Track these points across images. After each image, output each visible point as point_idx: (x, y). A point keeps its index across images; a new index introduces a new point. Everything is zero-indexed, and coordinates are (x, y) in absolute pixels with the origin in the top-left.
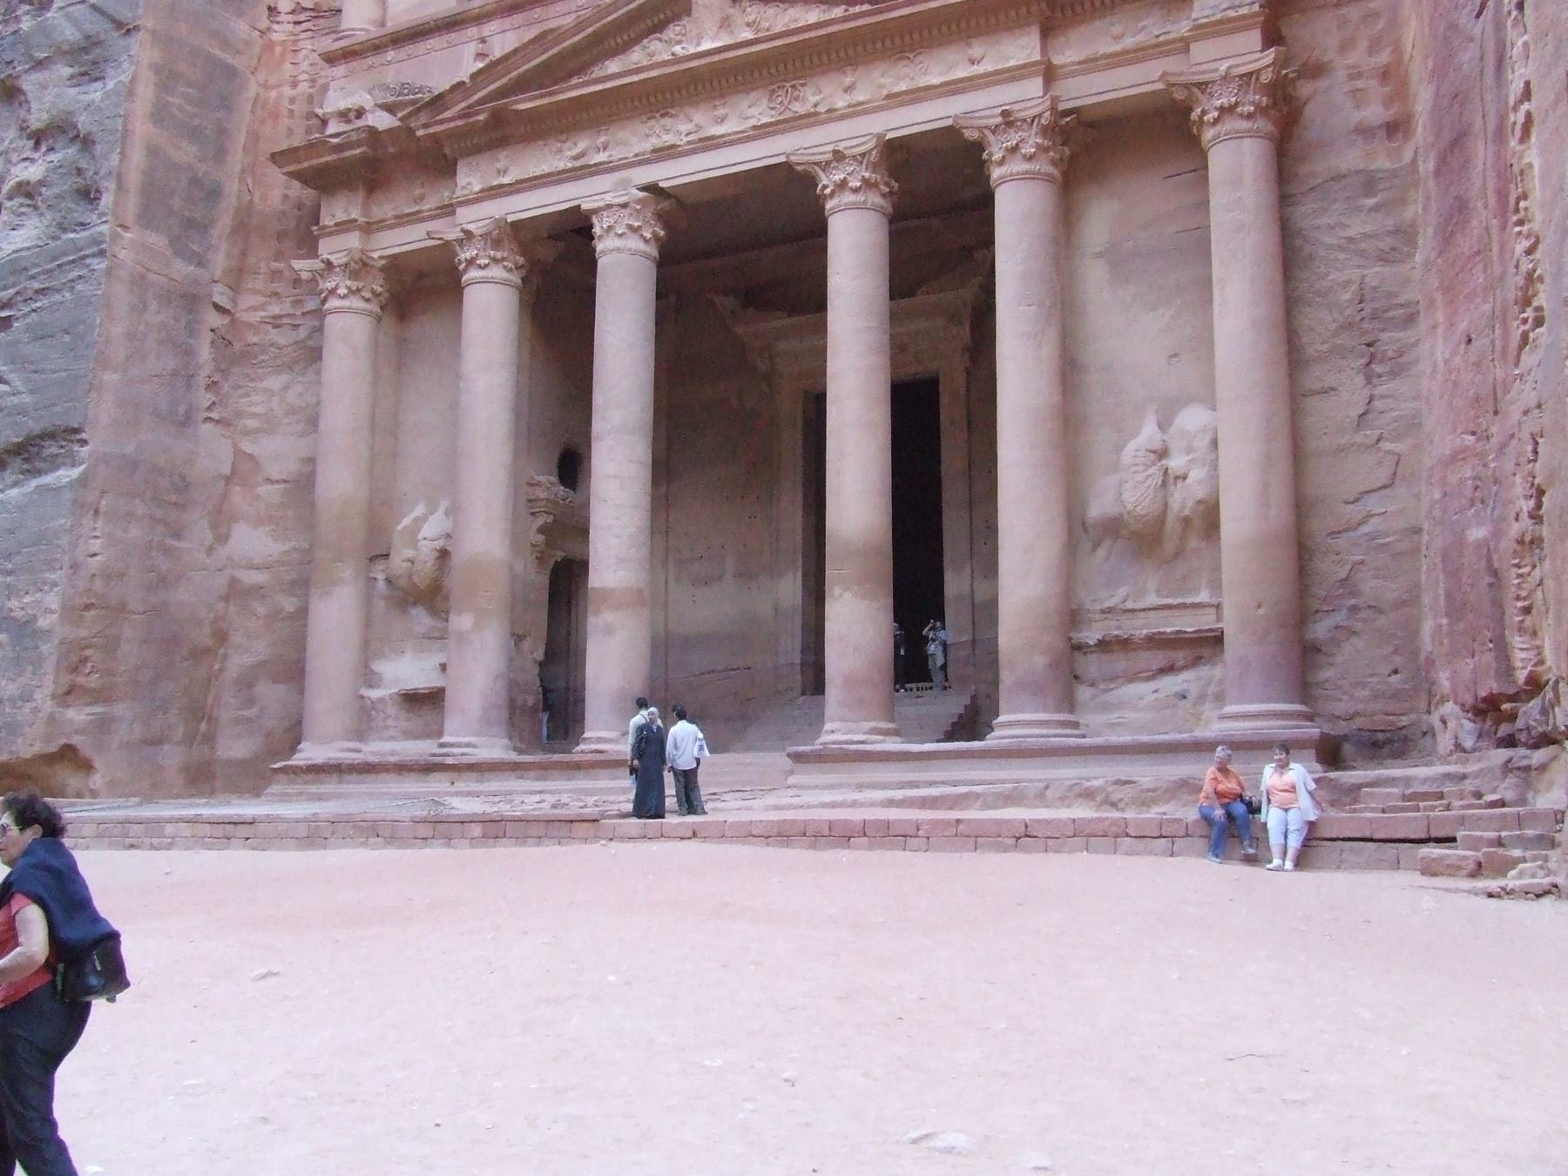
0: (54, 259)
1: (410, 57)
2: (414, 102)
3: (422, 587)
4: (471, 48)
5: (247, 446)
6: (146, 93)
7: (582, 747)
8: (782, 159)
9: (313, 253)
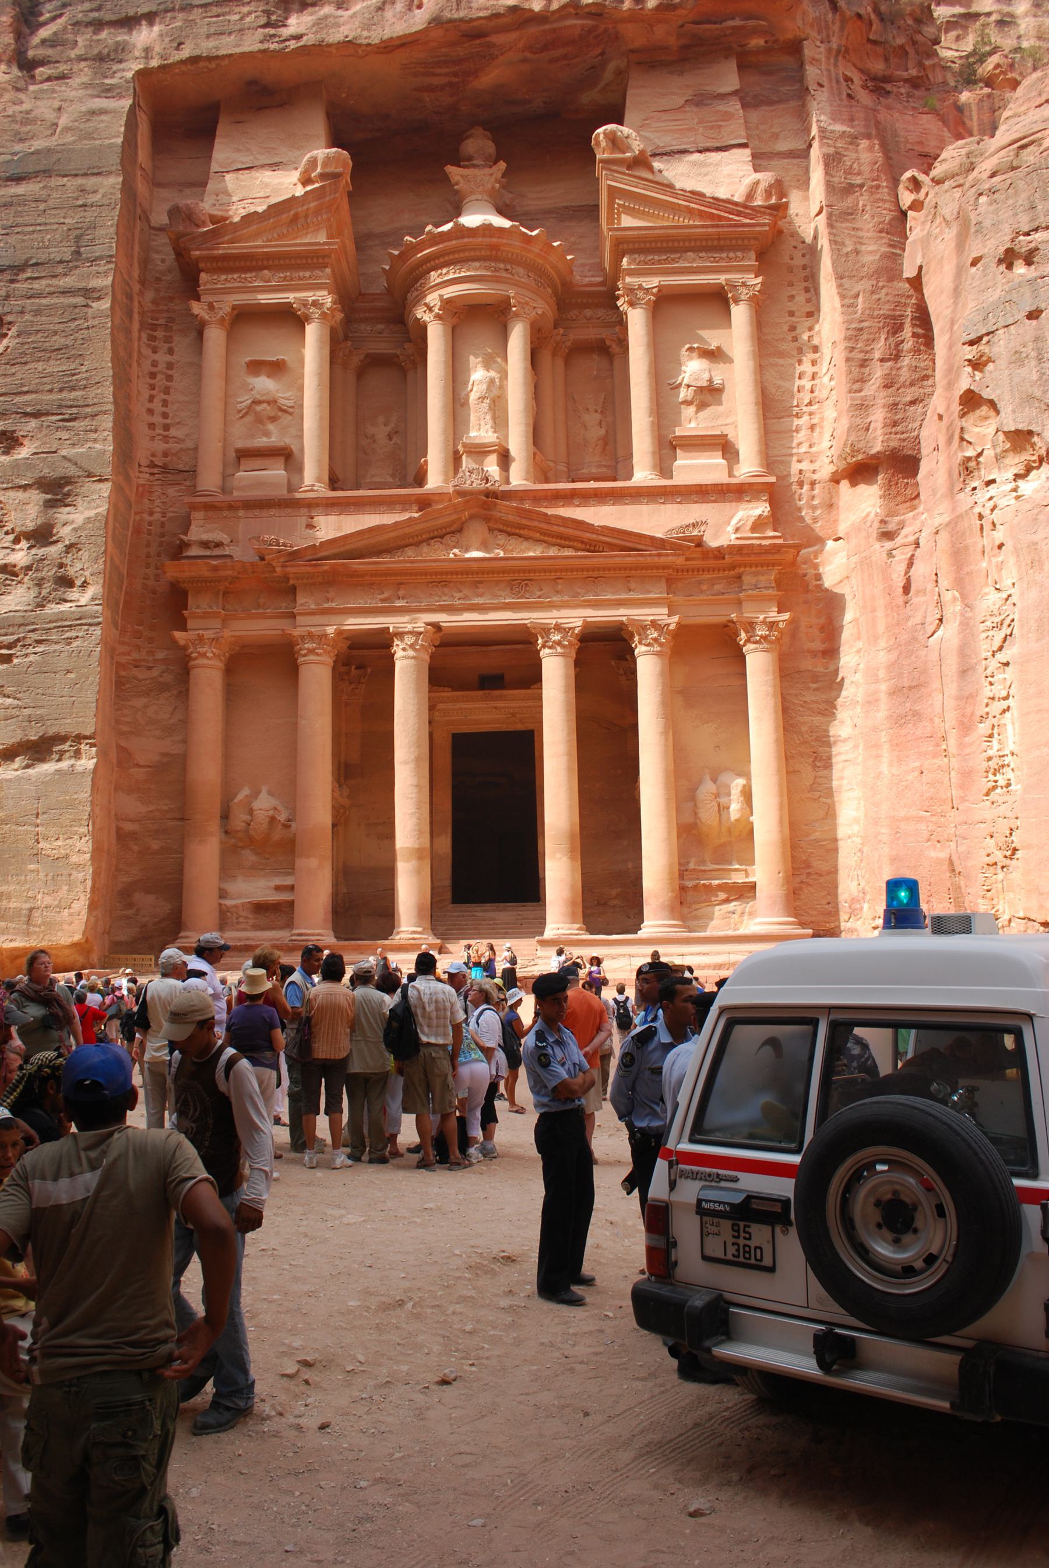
0: (50, 622)
1: (256, 517)
2: (280, 551)
4: (303, 521)
5: (124, 744)
7: (398, 937)
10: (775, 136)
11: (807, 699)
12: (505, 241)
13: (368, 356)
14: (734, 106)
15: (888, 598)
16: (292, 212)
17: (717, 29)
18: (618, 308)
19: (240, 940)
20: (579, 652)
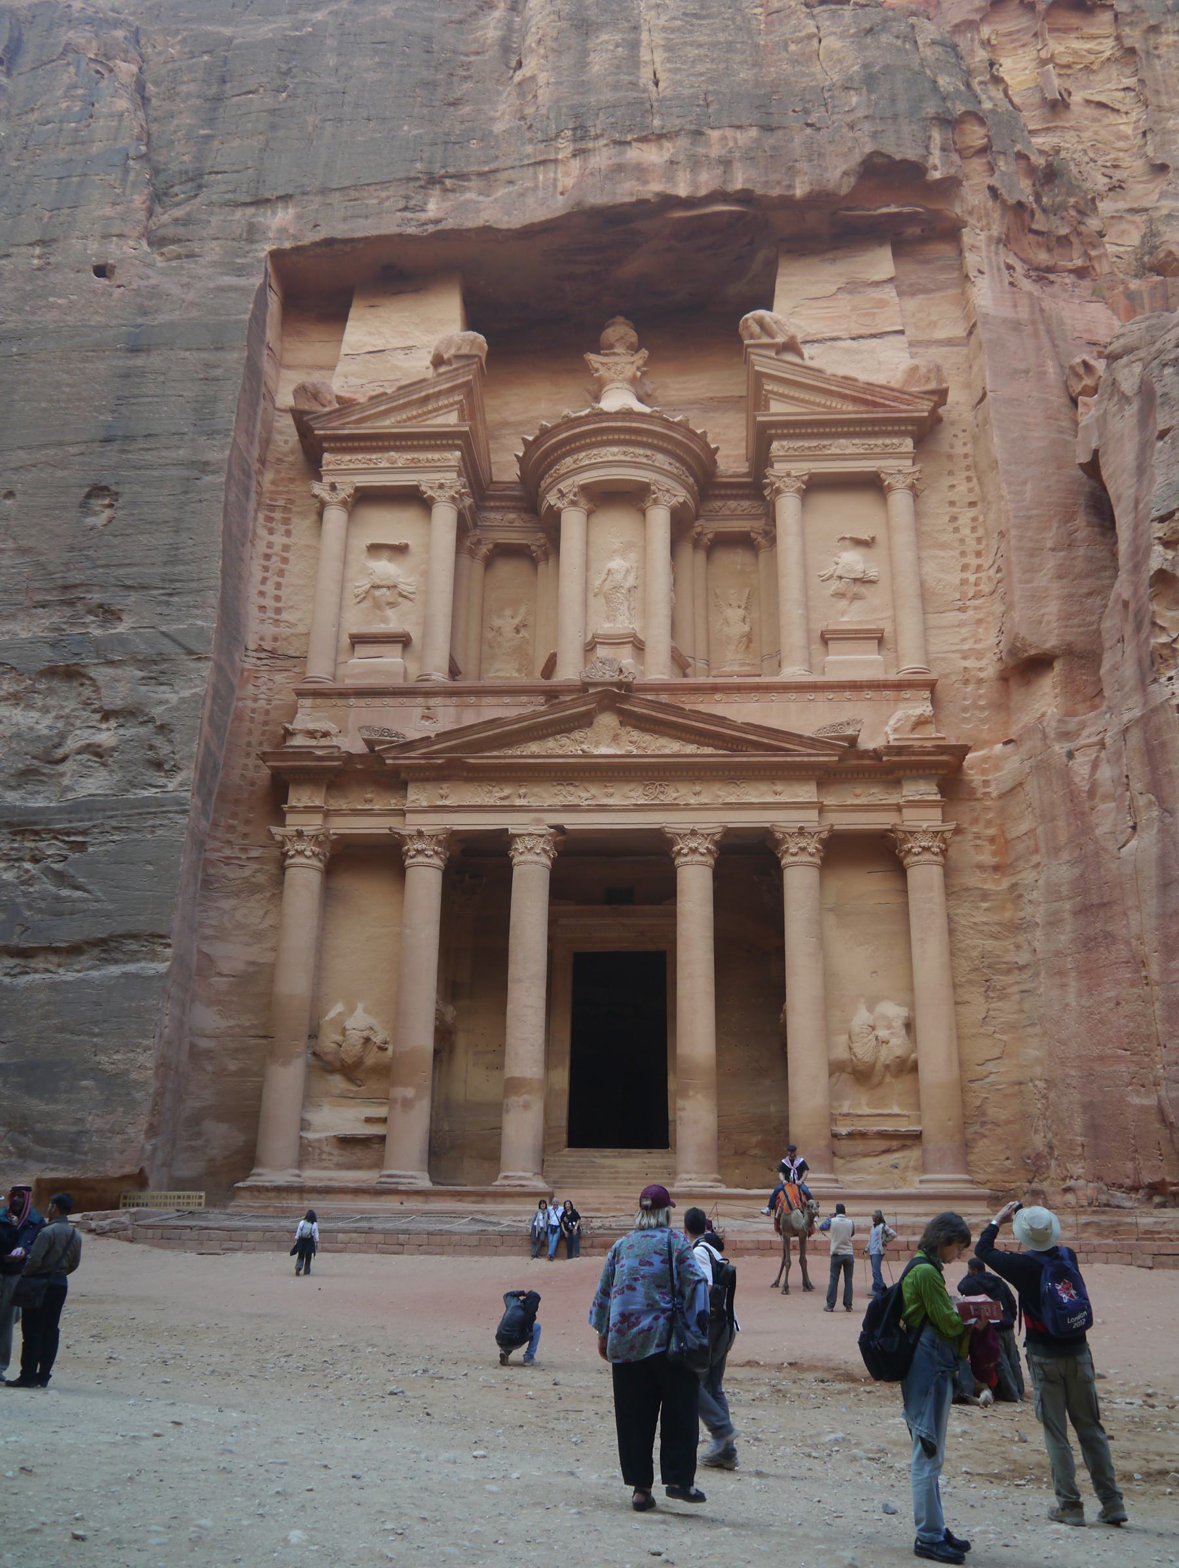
1: (368, 706)
2: (391, 742)
3: (349, 1061)
4: (419, 711)
5: (206, 949)
6: (208, 701)
8: (658, 826)
9: (281, 823)
10: (933, 324)
11: (974, 920)
12: (645, 426)
13: (497, 546)
14: (889, 293)
15: (1069, 805)
16: (423, 394)
17: (872, 216)
18: (763, 498)
19: (321, 1180)
20: (717, 862)
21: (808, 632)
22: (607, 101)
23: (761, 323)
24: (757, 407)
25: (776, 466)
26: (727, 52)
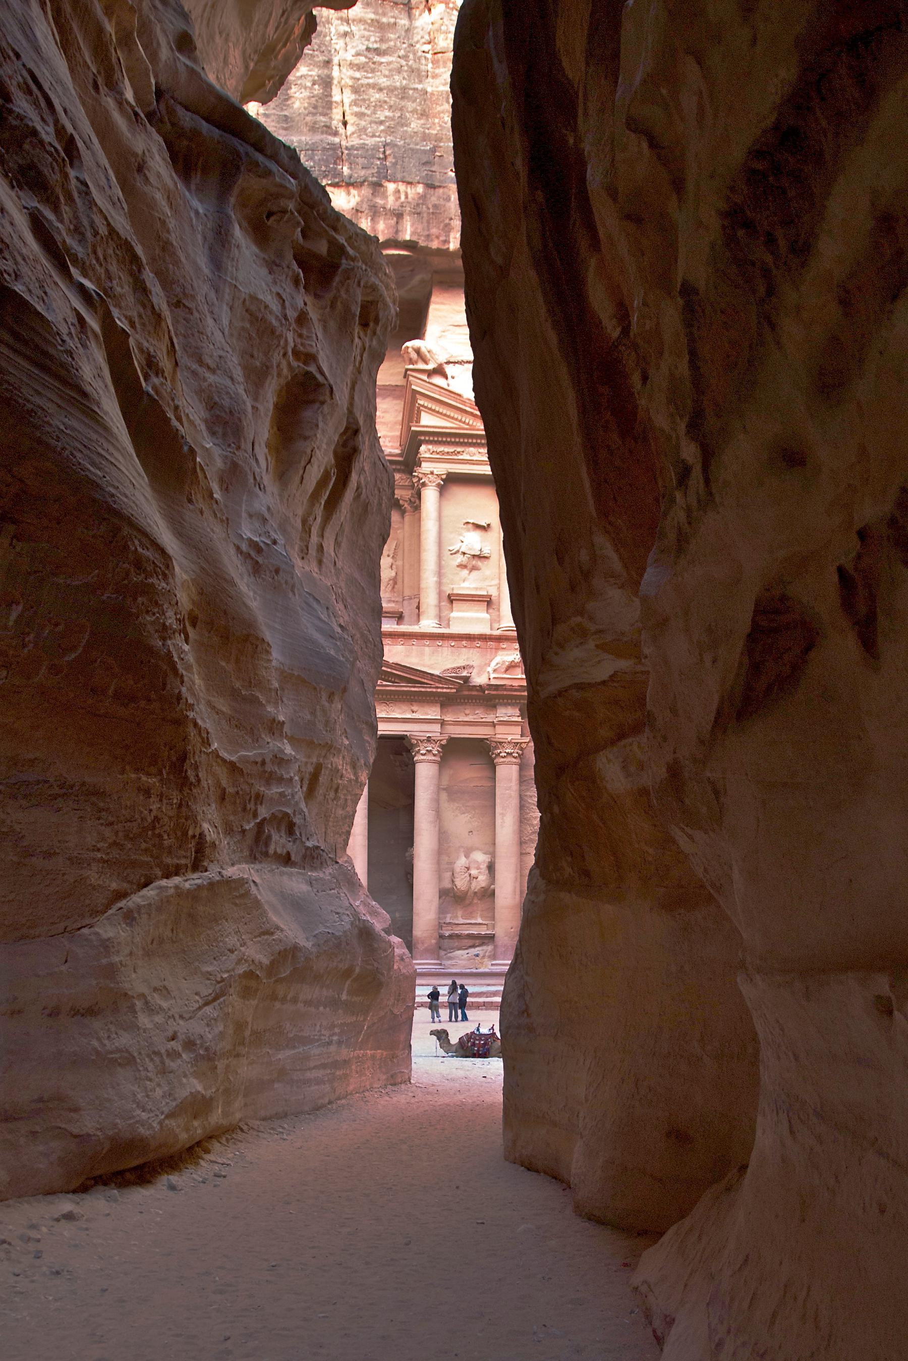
21: (440, 593)
22: (307, 144)
23: (418, 351)
24: (410, 420)
25: (424, 464)
26: (402, 98)
